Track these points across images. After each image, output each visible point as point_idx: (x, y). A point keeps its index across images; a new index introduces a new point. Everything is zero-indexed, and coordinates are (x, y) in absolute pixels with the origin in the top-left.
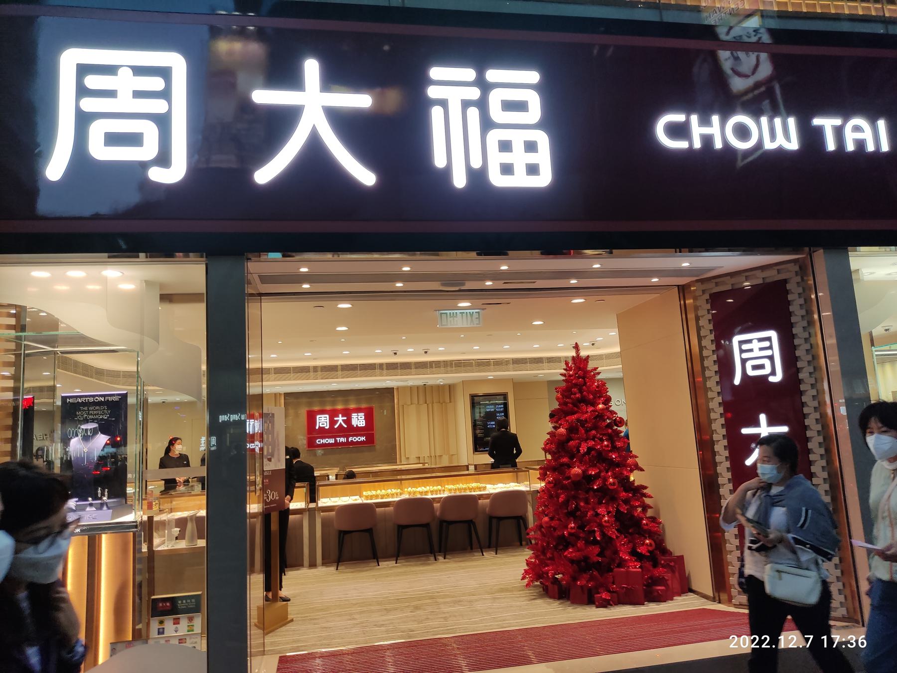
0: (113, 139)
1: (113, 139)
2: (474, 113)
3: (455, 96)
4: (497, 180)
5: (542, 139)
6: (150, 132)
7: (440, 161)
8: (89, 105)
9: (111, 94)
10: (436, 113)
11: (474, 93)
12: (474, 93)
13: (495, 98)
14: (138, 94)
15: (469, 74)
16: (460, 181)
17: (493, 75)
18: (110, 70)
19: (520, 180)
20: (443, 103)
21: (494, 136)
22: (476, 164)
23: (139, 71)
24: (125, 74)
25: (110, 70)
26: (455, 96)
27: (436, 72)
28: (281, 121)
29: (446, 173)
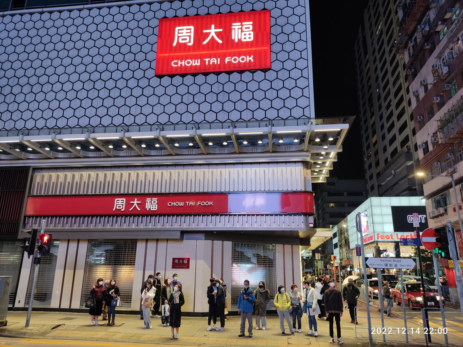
2: (240, 30)
3: (236, 28)
5: (252, 33)
6: (188, 38)
7: (233, 38)
8: (179, 35)
9: (182, 33)
10: (233, 31)
11: (240, 27)
12: (240, 27)
13: (244, 27)
14: (186, 33)
15: (240, 24)
16: (236, 41)
17: (244, 23)
18: (183, 30)
19: (248, 40)
20: (235, 29)
21: (243, 33)
22: (240, 38)
23: (187, 29)
24: (185, 30)
25: (183, 30)
27: (234, 24)
29: (234, 39)
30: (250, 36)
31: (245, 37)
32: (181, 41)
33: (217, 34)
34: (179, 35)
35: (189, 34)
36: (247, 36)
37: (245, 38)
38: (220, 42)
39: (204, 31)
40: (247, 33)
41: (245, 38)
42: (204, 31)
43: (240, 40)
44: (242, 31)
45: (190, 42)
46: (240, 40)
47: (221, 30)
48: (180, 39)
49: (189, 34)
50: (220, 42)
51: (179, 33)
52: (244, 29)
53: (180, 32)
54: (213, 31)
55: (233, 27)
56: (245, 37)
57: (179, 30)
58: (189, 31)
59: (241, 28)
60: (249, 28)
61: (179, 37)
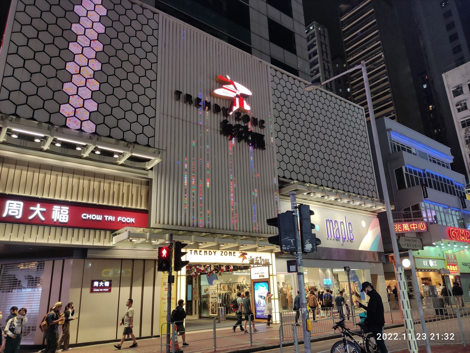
0: (12, 212)
1: (12, 212)
2: (59, 212)
3: (57, 210)
4: (60, 221)
5: (67, 216)
6: (17, 212)
8: (10, 208)
10: (54, 212)
11: (59, 210)
12: (59, 210)
13: (62, 210)
15: (59, 207)
19: (63, 221)
21: (61, 215)
26: (57, 210)
28: (33, 211)
30: (65, 218)
31: (62, 218)
32: (11, 214)
33: (42, 212)
34: (10, 208)
35: (18, 209)
36: (64, 218)
37: (62, 219)
38: (43, 219)
39: (32, 208)
40: (64, 216)
41: (62, 219)
42: (32, 208)
43: (58, 220)
44: (60, 213)
45: (18, 215)
46: (58, 220)
47: (44, 210)
48: (10, 211)
49: (18, 209)
50: (43, 219)
51: (9, 206)
52: (62, 212)
53: (11, 205)
54: (38, 210)
55: (54, 209)
56: (62, 218)
57: (10, 203)
58: (19, 206)
59: (60, 211)
60: (65, 212)
61: (9, 209)
